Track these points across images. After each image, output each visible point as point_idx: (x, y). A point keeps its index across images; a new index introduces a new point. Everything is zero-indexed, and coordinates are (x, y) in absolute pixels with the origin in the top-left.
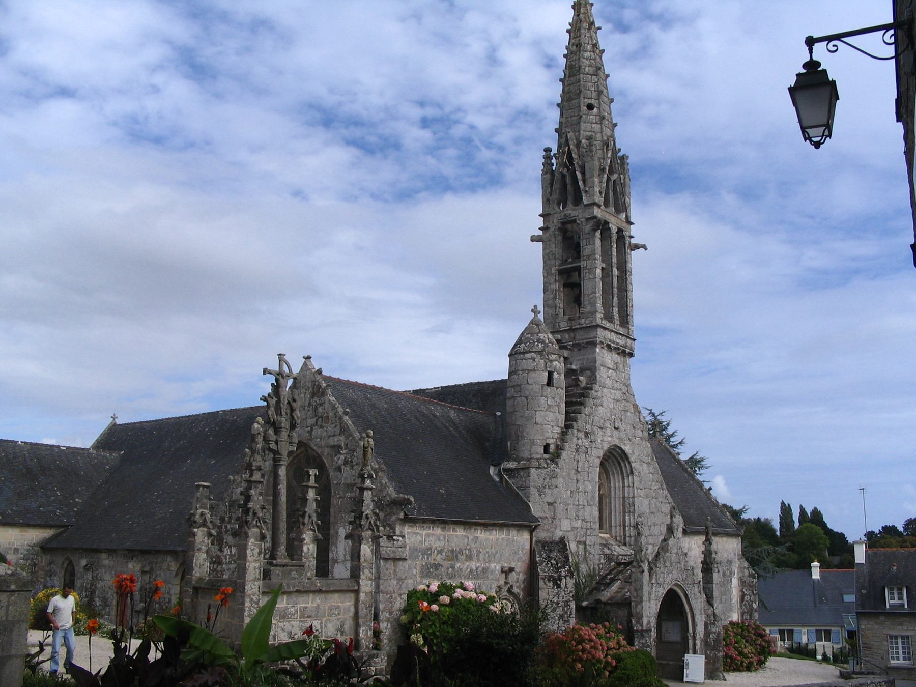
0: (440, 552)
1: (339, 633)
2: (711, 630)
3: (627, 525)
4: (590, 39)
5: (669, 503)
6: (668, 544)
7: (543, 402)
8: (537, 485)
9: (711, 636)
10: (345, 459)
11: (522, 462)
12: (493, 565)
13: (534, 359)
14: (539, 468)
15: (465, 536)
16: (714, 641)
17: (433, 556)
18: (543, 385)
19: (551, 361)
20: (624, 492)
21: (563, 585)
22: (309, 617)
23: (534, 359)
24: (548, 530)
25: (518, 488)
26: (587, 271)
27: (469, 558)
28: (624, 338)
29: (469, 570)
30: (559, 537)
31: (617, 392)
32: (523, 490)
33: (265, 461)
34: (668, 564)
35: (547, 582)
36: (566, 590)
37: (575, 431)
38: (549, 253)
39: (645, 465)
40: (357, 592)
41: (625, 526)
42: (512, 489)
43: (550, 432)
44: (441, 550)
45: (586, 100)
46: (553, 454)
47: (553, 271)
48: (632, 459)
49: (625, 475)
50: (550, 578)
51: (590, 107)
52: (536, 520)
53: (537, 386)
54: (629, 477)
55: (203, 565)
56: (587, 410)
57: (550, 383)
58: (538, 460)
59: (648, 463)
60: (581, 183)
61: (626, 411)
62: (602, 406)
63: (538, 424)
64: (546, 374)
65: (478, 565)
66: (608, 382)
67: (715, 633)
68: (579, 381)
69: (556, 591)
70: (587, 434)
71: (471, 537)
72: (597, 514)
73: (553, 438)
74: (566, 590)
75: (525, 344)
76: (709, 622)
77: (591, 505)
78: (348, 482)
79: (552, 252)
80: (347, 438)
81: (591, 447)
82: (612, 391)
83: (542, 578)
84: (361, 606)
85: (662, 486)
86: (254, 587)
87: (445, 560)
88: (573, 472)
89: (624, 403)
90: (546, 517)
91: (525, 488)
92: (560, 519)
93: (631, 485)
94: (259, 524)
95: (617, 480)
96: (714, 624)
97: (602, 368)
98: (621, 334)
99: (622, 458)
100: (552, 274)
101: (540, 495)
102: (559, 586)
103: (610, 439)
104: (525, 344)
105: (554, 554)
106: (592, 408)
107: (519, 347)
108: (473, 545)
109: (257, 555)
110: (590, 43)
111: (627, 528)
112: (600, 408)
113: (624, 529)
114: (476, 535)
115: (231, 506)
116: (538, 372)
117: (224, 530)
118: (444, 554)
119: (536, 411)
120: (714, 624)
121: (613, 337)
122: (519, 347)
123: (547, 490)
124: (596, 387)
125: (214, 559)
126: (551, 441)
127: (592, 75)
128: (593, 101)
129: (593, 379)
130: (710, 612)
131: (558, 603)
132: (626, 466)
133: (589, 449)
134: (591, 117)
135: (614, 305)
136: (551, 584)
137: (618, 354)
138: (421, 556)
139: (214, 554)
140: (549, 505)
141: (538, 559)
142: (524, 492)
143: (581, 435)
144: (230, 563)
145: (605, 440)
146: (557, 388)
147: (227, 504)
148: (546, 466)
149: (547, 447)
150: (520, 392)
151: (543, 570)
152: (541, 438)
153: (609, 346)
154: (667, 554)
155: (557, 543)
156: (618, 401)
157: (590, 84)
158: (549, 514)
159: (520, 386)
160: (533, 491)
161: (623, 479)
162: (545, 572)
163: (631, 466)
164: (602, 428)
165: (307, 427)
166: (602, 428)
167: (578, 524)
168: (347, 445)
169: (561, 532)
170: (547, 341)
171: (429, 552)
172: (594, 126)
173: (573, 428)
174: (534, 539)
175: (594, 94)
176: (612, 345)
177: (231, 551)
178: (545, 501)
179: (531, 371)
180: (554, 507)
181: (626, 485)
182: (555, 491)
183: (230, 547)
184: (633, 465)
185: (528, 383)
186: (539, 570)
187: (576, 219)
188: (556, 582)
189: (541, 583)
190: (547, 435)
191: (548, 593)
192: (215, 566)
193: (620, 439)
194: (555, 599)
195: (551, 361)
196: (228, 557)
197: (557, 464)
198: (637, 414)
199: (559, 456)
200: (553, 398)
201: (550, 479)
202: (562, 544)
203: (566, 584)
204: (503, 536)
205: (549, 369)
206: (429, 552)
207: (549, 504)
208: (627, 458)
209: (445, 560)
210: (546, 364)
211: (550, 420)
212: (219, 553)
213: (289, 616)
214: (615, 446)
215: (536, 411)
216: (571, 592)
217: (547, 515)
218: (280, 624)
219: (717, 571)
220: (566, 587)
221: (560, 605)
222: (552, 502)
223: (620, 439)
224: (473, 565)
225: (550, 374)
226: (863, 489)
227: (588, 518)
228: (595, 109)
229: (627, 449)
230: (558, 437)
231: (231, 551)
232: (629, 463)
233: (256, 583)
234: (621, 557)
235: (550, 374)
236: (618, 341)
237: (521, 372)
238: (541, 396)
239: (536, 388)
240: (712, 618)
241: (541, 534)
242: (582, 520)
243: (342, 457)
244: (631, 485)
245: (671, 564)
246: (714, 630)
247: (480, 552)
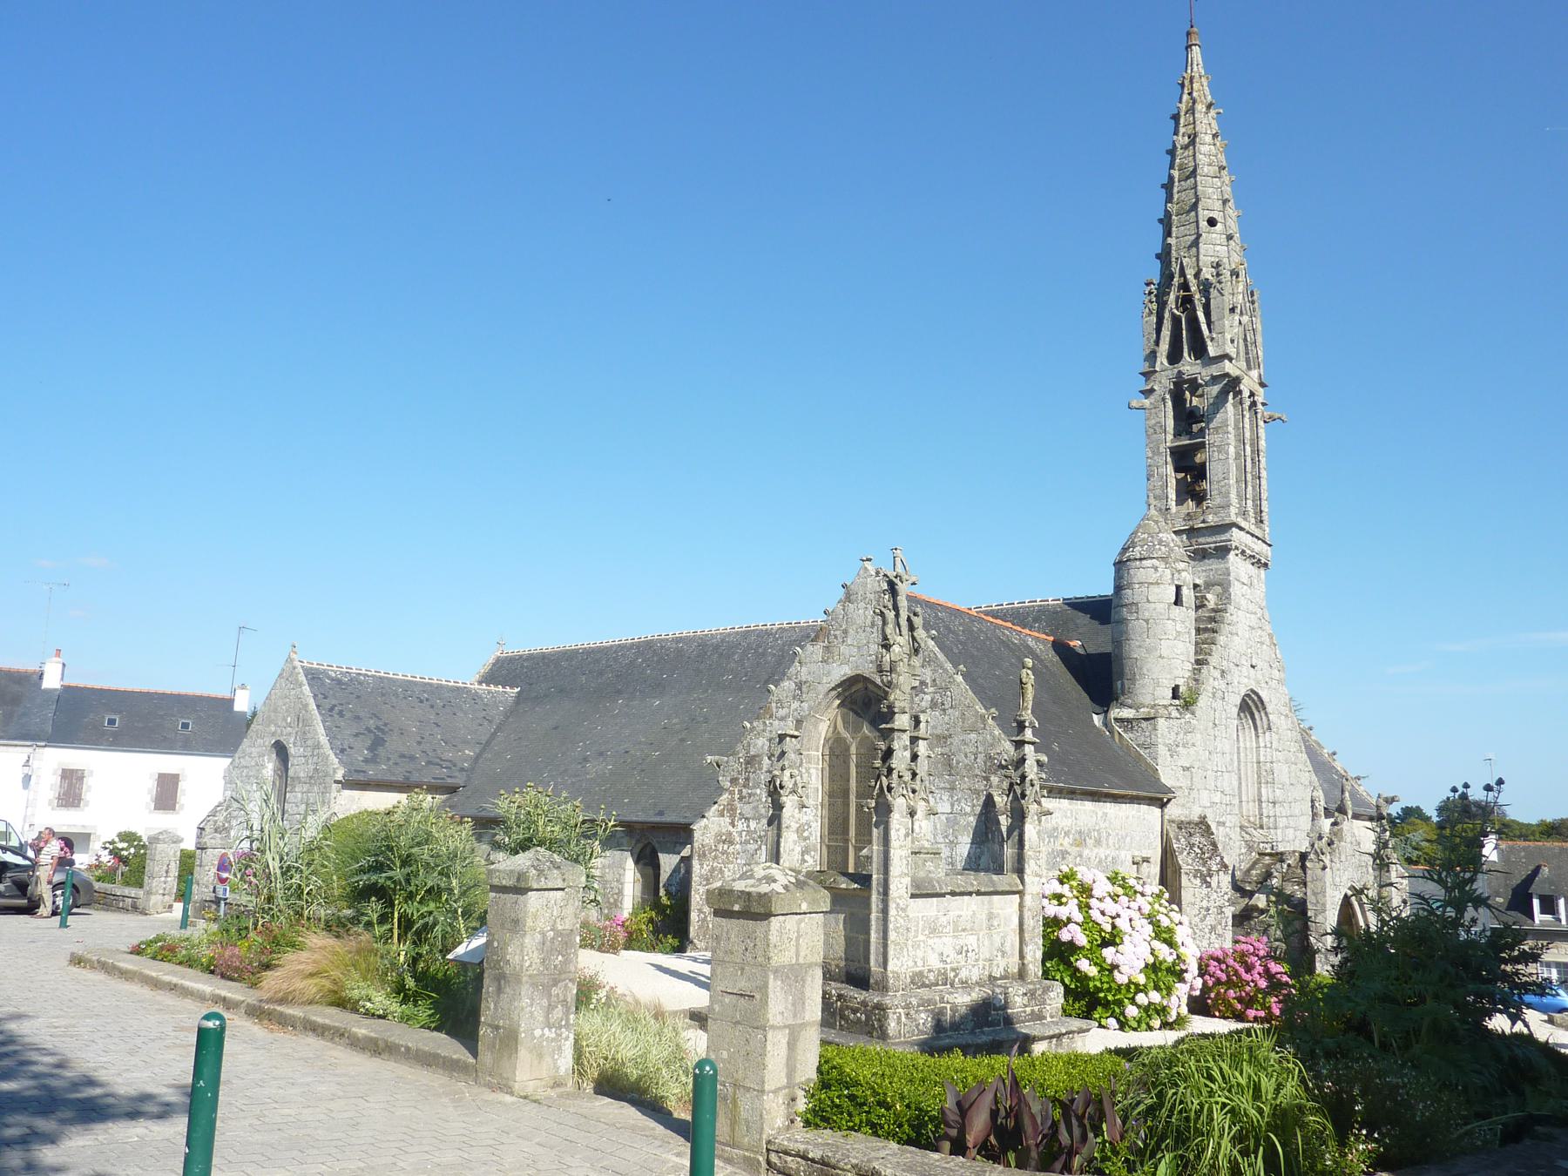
0: (1067, 834)
1: (1000, 954)
3: (1263, 799)
4: (1208, 127)
6: (1342, 828)
7: (1170, 627)
8: (1167, 742)
10: (932, 700)
11: (1142, 710)
12: (1123, 853)
13: (1156, 569)
14: (1170, 718)
15: (1093, 811)
17: (1061, 841)
18: (1169, 605)
19: (1179, 572)
20: (1258, 755)
21: (1214, 885)
22: (964, 930)
23: (1156, 569)
24: (1183, 805)
25: (1137, 745)
26: (1215, 449)
27: (1098, 842)
28: (1260, 541)
29: (1097, 860)
30: (1198, 815)
31: (1253, 616)
32: (1145, 748)
33: (802, 702)
34: (1343, 858)
35: (1192, 879)
36: (1219, 890)
37: (1212, 668)
38: (1155, 425)
39: (1283, 717)
40: (1021, 893)
41: (1260, 801)
42: (1128, 747)
43: (1180, 669)
44: (1068, 831)
45: (1206, 212)
46: (1184, 699)
47: (1162, 449)
49: (1260, 731)
50: (1197, 874)
51: (1212, 222)
52: (1169, 791)
53: (1162, 605)
54: (1265, 733)
55: (793, 850)
56: (1221, 639)
57: (1178, 601)
58: (1165, 707)
59: (1286, 716)
60: (1204, 327)
61: (1262, 643)
62: (1237, 634)
63: (1163, 658)
64: (1174, 588)
65: (1108, 852)
66: (1243, 602)
68: (1206, 599)
69: (1205, 891)
71: (1100, 814)
72: (1235, 784)
73: (1183, 677)
74: (1219, 890)
75: (1142, 546)
77: (1229, 772)
78: (938, 732)
79: (1159, 423)
80: (934, 671)
82: (1248, 615)
83: (1186, 873)
84: (1027, 914)
85: (1300, 746)
86: (900, 886)
87: (1072, 845)
88: (1211, 724)
89: (1260, 631)
90: (1181, 787)
91: (1150, 746)
92: (1198, 790)
93: (1269, 745)
94: (905, 792)
95: (1247, 738)
97: (1236, 583)
98: (1257, 537)
99: (1257, 707)
100: (1159, 454)
101: (1172, 756)
102: (1209, 885)
103: (1246, 680)
104: (1142, 546)
105: (1196, 839)
106: (1227, 637)
107: (1133, 551)
108: (1103, 826)
109: (903, 838)
110: (1209, 132)
111: (1264, 805)
112: (1235, 637)
113: (1260, 805)
114: (1105, 811)
115: (747, 763)
116: (1162, 586)
117: (737, 796)
118: (1071, 836)
119: (1161, 640)
121: (1248, 539)
122: (1133, 551)
123: (1180, 749)
124: (1231, 608)
125: (724, 838)
126: (1180, 682)
127: (1213, 177)
128: (1214, 215)
129: (1225, 596)
131: (1208, 909)
132: (1261, 719)
133: (1226, 694)
134: (1214, 235)
135: (1248, 496)
136: (1198, 881)
138: (1047, 840)
139: (724, 831)
140: (1184, 770)
141: (1175, 846)
142: (1148, 751)
143: (1217, 674)
144: (747, 842)
145: (1242, 682)
147: (741, 760)
148: (1179, 717)
149: (1175, 690)
150: (1137, 613)
151: (1185, 861)
152: (1169, 676)
153: (1243, 552)
155: (1197, 824)
156: (1253, 629)
157: (1211, 190)
158: (1184, 783)
159: (1136, 604)
160: (1162, 750)
161: (1257, 736)
162: (1188, 865)
163: (1269, 720)
164: (1238, 666)
165: (870, 655)
166: (1238, 666)
167: (1217, 798)
168: (934, 680)
169: (1200, 809)
170: (1172, 545)
171: (1056, 834)
172: (1218, 248)
173: (1208, 664)
174: (1166, 817)
175: (1218, 205)
177: (748, 826)
178: (1180, 764)
179: (1152, 584)
180: (1192, 773)
181: (1262, 744)
182: (1192, 750)
183: (747, 819)
184: (1271, 717)
185: (1148, 601)
186: (1180, 862)
187: (1196, 378)
188: (1205, 880)
189: (1184, 879)
190: (1177, 673)
191: (1194, 895)
192: (726, 847)
193: (1258, 682)
194: (1205, 904)
195: (1179, 572)
196: (744, 833)
197: (1193, 713)
198: (1272, 647)
199: (1194, 702)
200: (1183, 622)
201: (1185, 734)
202: (1203, 825)
203: (1219, 883)
205: (1177, 583)
206: (1056, 834)
207: (1186, 769)
208: (1265, 709)
209: (1072, 845)
210: (1173, 575)
211: (1179, 652)
212: (730, 828)
213: (941, 929)
215: (1161, 640)
216: (1226, 893)
217: (1181, 785)
218: (930, 942)
220: (1218, 887)
221: (1210, 912)
222: (1188, 766)
223: (1258, 682)
224: (1102, 852)
225: (1178, 588)
226: (1490, 759)
227: (1227, 791)
228: (1219, 224)
229: (1263, 694)
230: (1189, 677)
231: (748, 826)
232: (1266, 714)
233: (903, 880)
234: (1262, 845)
235: (1178, 588)
236: (1253, 546)
237: (1137, 586)
238: (1168, 619)
239: (1160, 607)
241: (1173, 811)
243: (928, 698)
244: (1269, 745)
247: (1109, 835)
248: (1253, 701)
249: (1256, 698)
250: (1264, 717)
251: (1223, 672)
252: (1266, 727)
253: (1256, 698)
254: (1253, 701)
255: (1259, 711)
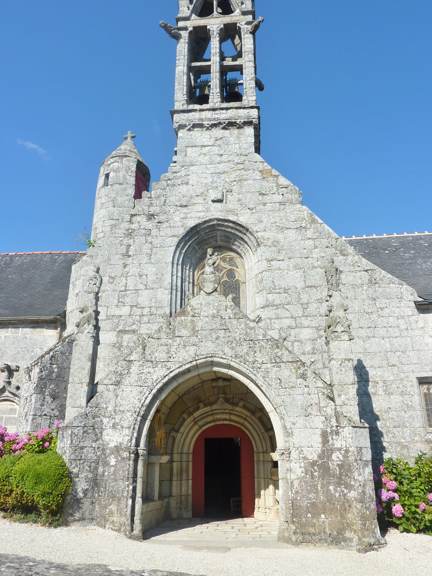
2: (333, 445)
5: (366, 271)
9: (334, 457)
16: (338, 465)
48: (253, 228)
67: (339, 450)
70: (151, 217)
76: (329, 430)
81: (159, 228)
96: (337, 433)
99: (240, 231)
120: (337, 433)
130: (330, 411)
137: (224, 128)
146: (112, 185)
154: (183, 318)
163: (255, 238)
164: (186, 206)
166: (186, 206)
176: (204, 123)
204: (6, 334)
208: (247, 230)
214: (218, 220)
219: (346, 337)
232: (251, 233)
236: (217, 116)
240: (334, 420)
242: (132, 306)
245: (195, 332)
246: (338, 444)
248: (232, 228)
249: (231, 225)
250: (251, 237)
251: (153, 215)
252: (256, 244)
253: (231, 225)
254: (232, 228)
255: (245, 234)
